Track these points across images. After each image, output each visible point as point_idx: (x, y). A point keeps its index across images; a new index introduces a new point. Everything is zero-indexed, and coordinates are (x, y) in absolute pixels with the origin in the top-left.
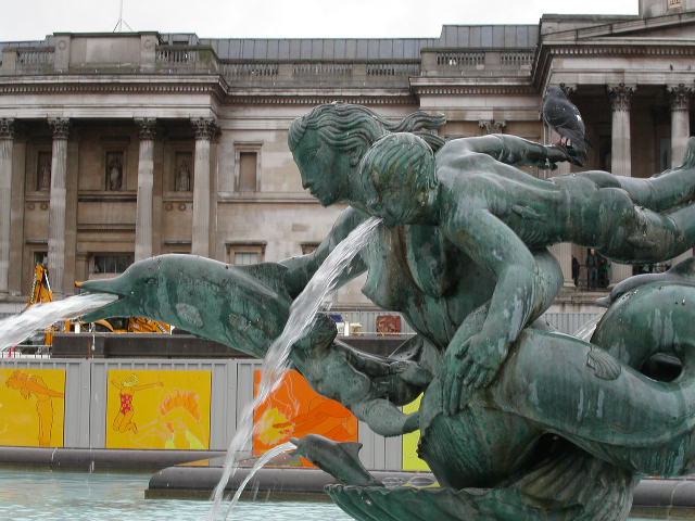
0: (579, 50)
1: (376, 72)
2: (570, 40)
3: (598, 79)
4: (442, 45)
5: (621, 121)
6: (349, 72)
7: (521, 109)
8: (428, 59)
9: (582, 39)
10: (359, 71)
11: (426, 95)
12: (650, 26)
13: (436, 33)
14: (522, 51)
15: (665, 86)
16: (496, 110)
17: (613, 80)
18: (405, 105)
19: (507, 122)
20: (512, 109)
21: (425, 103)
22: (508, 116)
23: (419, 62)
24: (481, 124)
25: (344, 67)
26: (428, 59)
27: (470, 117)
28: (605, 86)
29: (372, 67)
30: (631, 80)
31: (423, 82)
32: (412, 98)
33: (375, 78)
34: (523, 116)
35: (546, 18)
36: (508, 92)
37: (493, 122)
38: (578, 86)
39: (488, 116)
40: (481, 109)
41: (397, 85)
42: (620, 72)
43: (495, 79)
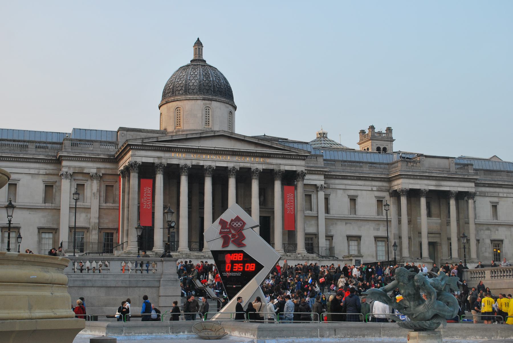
0: (143, 147)
1: (39, 147)
2: (139, 142)
3: (151, 160)
4: (72, 137)
5: (159, 179)
6: (27, 146)
7: (109, 169)
8: (67, 143)
9: (145, 143)
10: (31, 146)
11: (66, 160)
12: (173, 139)
13: (70, 131)
14: (110, 143)
15: (179, 165)
16: (97, 168)
17: (157, 161)
18: (55, 163)
19: (103, 174)
20: (105, 168)
21: (64, 163)
22: (103, 171)
23: (61, 144)
24: (91, 174)
25: (25, 144)
26: (67, 143)
27: (86, 171)
28: (154, 163)
29: (38, 145)
30: (164, 162)
31: (65, 154)
32: (58, 161)
33: (39, 150)
34: (110, 172)
35: (121, 129)
36: (104, 160)
37: (96, 174)
38: (142, 162)
39: (94, 171)
40: (91, 168)
41: (50, 153)
42: (159, 158)
43: (98, 154)
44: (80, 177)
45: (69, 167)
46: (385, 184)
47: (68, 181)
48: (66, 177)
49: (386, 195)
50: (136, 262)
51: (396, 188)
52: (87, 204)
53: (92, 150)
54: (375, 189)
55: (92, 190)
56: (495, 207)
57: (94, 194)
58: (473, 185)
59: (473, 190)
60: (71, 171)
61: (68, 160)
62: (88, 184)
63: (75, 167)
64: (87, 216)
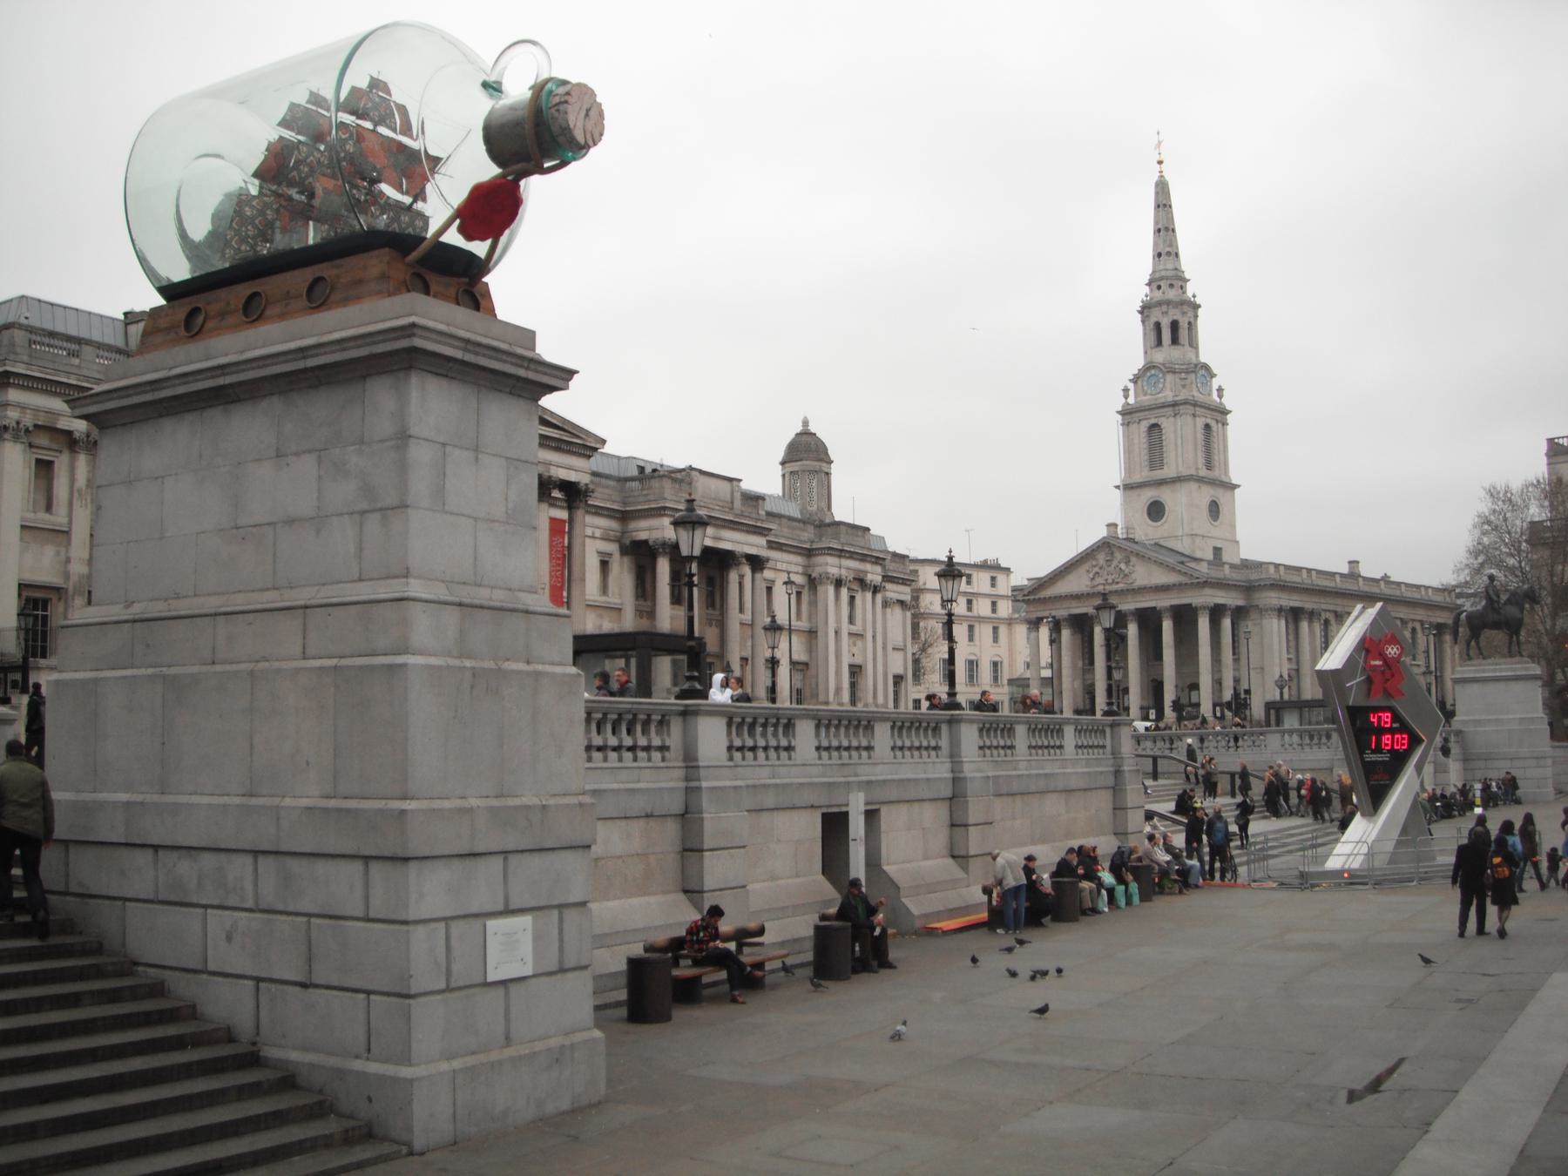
44: (43, 440)
45: (23, 408)
46: (613, 525)
47: (19, 447)
48: (16, 438)
49: (613, 548)
50: (605, 714)
51: (643, 536)
52: (59, 518)
53: (79, 367)
54: (598, 533)
55: (72, 480)
56: (769, 589)
57: (79, 491)
58: (762, 541)
59: (764, 553)
60: (28, 421)
61: (22, 387)
62: (61, 462)
63: (37, 410)
64: (58, 553)
